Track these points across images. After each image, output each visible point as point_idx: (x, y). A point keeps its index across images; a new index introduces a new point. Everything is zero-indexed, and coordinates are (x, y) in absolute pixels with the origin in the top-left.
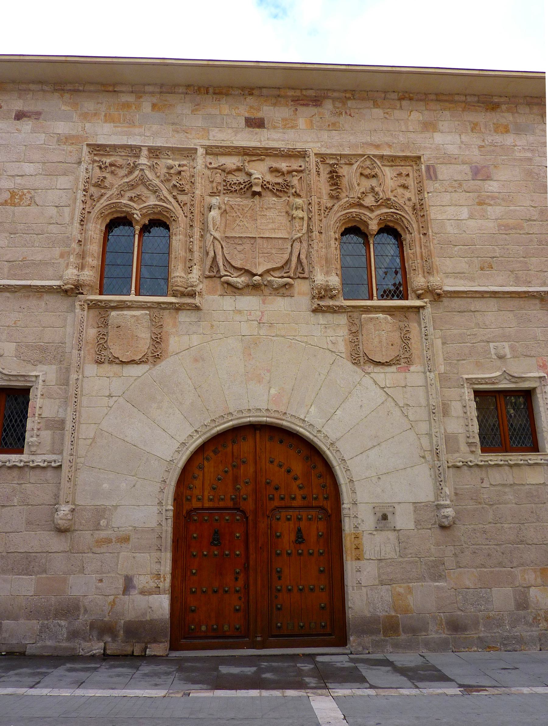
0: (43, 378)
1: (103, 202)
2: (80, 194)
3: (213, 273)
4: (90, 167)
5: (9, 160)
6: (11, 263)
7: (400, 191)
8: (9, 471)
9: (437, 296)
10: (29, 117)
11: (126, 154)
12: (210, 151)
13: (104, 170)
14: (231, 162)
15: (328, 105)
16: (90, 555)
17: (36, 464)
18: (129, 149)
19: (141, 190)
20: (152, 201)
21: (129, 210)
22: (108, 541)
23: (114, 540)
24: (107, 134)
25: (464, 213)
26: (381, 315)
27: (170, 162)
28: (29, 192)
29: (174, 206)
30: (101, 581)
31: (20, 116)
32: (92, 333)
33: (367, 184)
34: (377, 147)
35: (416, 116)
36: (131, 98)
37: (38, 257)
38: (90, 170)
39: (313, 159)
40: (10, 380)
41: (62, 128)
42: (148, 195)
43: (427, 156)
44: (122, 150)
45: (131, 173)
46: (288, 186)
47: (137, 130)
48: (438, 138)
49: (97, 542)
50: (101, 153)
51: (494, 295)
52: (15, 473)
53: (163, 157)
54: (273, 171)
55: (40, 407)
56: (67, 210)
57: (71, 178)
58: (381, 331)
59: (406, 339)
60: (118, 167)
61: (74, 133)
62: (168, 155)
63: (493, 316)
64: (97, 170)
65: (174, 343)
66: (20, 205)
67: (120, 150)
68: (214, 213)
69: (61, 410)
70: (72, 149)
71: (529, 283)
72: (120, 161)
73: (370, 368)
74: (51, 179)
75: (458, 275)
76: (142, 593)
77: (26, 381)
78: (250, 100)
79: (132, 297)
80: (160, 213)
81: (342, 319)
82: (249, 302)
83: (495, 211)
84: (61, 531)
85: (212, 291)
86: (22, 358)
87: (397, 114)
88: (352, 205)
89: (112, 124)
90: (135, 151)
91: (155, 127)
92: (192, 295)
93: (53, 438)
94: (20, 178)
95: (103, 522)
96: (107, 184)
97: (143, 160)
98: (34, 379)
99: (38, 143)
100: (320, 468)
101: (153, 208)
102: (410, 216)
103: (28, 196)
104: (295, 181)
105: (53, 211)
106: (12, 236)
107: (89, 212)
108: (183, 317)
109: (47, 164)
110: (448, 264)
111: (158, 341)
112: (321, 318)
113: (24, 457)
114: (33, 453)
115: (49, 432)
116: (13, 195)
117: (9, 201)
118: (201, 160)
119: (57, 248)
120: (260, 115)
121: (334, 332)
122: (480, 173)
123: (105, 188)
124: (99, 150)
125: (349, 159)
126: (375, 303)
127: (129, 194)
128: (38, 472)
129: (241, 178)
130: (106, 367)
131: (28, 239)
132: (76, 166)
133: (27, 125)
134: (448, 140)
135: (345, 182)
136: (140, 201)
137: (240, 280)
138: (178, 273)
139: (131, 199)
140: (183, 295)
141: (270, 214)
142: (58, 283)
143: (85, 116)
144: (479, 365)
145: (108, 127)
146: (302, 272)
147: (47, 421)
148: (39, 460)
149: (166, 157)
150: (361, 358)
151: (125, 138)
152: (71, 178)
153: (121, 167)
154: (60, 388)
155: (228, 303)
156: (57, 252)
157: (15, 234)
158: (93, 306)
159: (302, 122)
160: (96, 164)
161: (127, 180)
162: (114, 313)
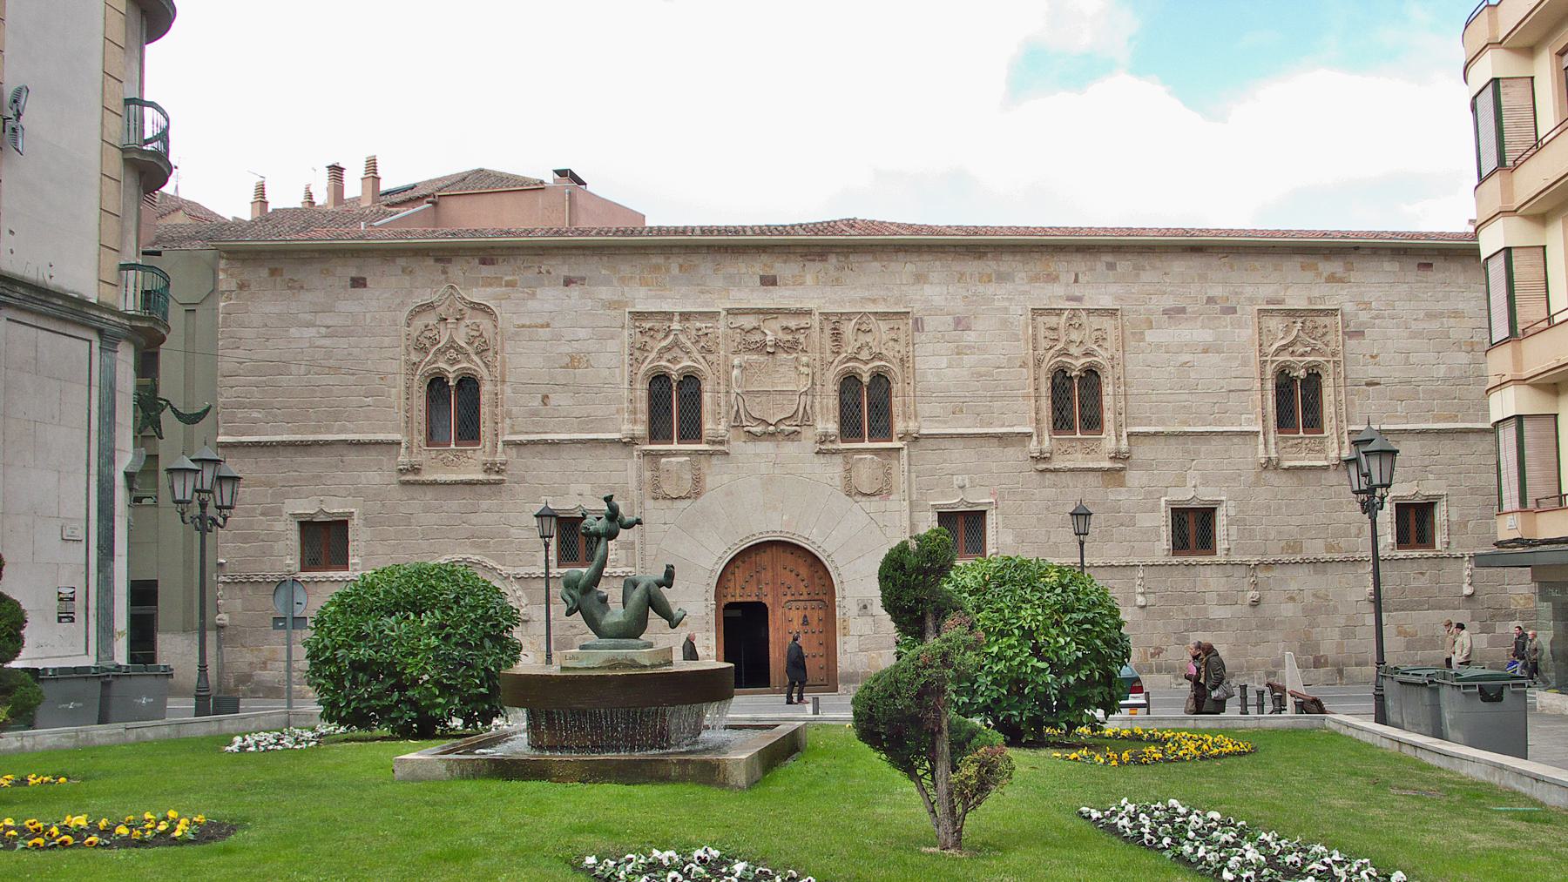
1: (645, 367)
2: (627, 358)
3: (737, 424)
7: (891, 343)
9: (915, 439)
12: (729, 312)
14: (748, 322)
15: (833, 259)
20: (686, 363)
24: (644, 299)
25: (944, 363)
26: (869, 456)
27: (698, 325)
29: (703, 366)
31: (568, 282)
32: (648, 474)
33: (863, 338)
34: (874, 301)
35: (910, 267)
36: (659, 260)
37: (600, 413)
39: (817, 318)
41: (605, 293)
43: (917, 308)
45: (666, 336)
46: (797, 342)
48: (928, 290)
51: (961, 436)
54: (785, 328)
58: (866, 470)
59: (887, 474)
63: (959, 455)
65: (709, 481)
68: (736, 372)
71: (990, 424)
72: (657, 325)
73: (858, 498)
75: (932, 418)
78: (764, 257)
79: (675, 446)
81: (838, 459)
82: (765, 447)
83: (969, 360)
85: (737, 438)
87: (893, 266)
88: (849, 360)
90: (669, 316)
91: (684, 289)
92: (721, 443)
97: (676, 326)
100: (821, 573)
102: (896, 368)
104: (802, 339)
108: (715, 460)
110: (925, 409)
111: (697, 480)
112: (822, 459)
116: (572, 358)
118: (722, 323)
120: (772, 272)
121: (833, 470)
122: (961, 324)
125: (848, 316)
126: (867, 444)
127: (667, 356)
129: (757, 337)
133: (575, 291)
134: (934, 292)
135: (845, 337)
137: (758, 429)
138: (708, 426)
140: (714, 442)
141: (782, 370)
143: (622, 280)
144: (943, 494)
145: (643, 291)
146: (807, 420)
150: (852, 491)
155: (752, 448)
156: (613, 408)
158: (646, 454)
159: (809, 279)
161: (664, 343)
162: (663, 460)
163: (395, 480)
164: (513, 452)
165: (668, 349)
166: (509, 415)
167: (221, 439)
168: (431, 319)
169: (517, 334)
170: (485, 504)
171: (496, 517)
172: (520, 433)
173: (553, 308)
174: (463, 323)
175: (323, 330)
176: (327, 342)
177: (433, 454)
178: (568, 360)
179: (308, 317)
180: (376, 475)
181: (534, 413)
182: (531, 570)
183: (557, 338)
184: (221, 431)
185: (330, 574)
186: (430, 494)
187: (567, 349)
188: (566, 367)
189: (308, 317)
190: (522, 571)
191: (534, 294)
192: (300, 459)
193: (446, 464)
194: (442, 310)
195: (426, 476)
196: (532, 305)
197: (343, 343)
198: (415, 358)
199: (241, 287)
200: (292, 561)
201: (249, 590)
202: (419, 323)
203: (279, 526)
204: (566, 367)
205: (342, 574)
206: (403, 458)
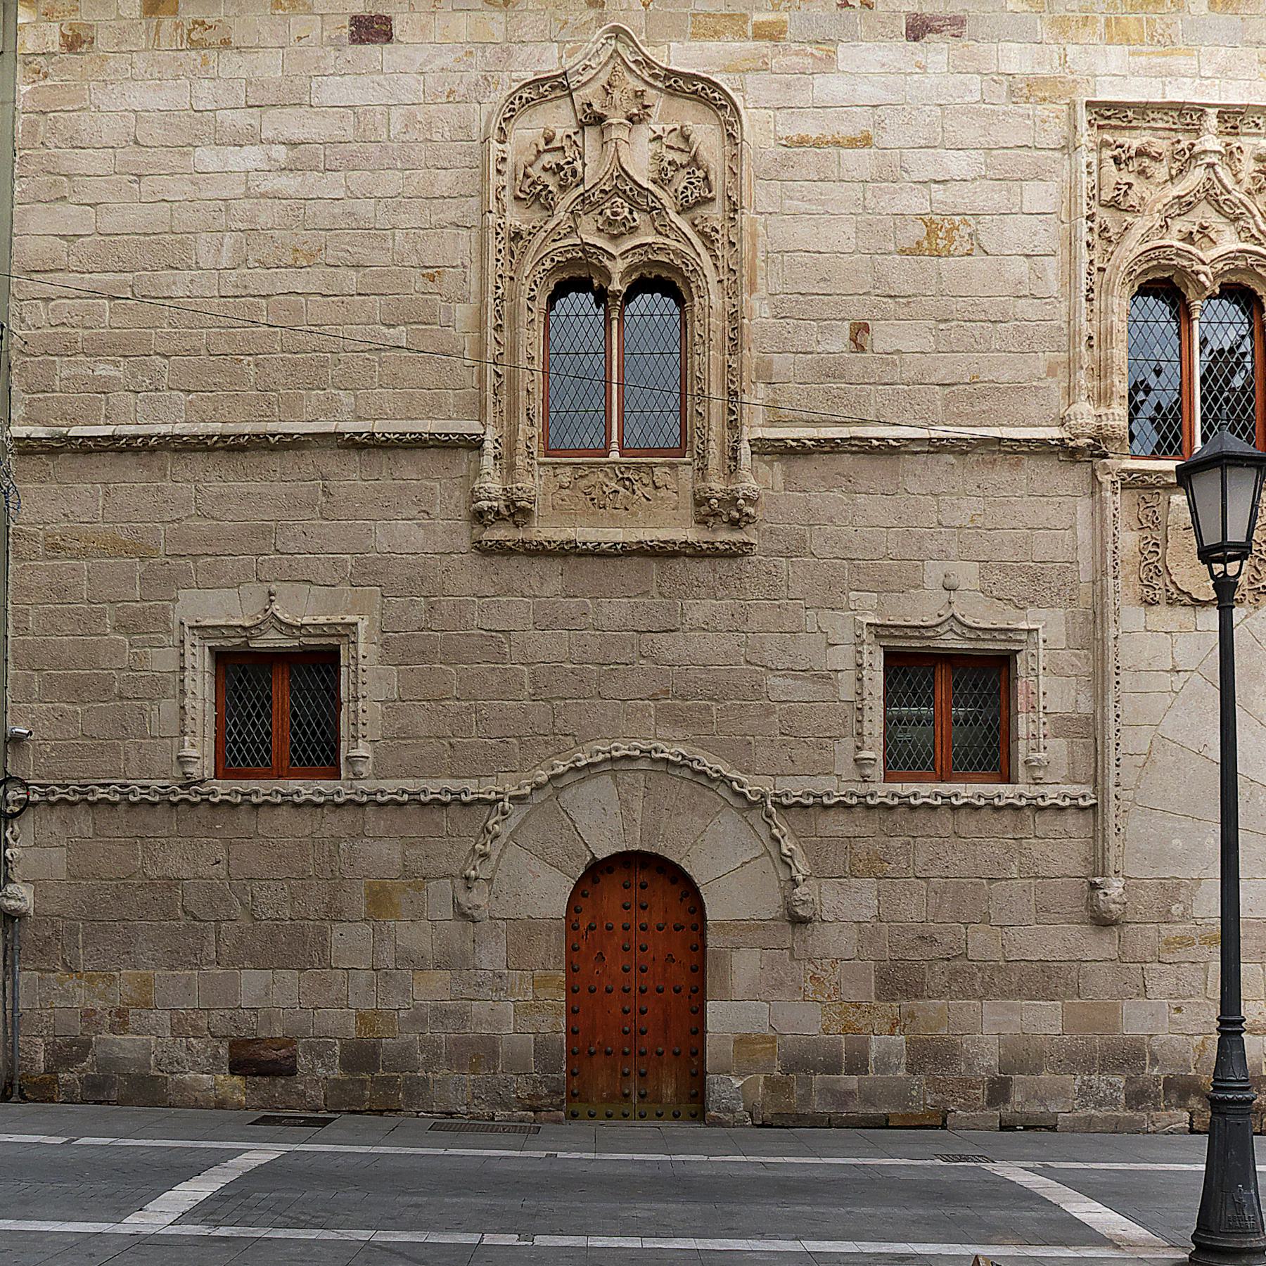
0: (1045, 633)
1: (1132, 247)
4: (1093, 158)
5: (911, 144)
6: (947, 390)
8: (995, 816)
10: (939, 31)
11: (1167, 126)
13: (1123, 166)
16: (1155, 965)
17: (1048, 802)
18: (1175, 114)
19: (1205, 214)
20: (1229, 242)
21: (1186, 263)
22: (1185, 942)
23: (1196, 940)
24: (1121, 76)
28: (966, 223)
30: (1179, 1010)
31: (918, 29)
32: (1129, 540)
38: (1094, 167)
40: (978, 639)
42: (1221, 227)
44: (1159, 116)
47: (1180, 62)
49: (1167, 943)
50: (1113, 122)
52: (1007, 818)
53: (1245, 130)
55: (1046, 692)
56: (1051, 266)
57: (1053, 186)
60: (1154, 158)
61: (1045, 71)
62: (1257, 125)
64: (1110, 166)
66: (950, 255)
67: (1155, 115)
69: (1081, 698)
70: (1046, 113)
74: (1009, 191)
77: (1009, 640)
80: (1250, 270)
84: (1102, 922)
86: (995, 593)
89: (1126, 48)
93: (1071, 753)
94: (941, 187)
95: (1176, 909)
96: (1133, 199)
98: (1024, 637)
99: (967, 99)
101: (1235, 258)
103: (965, 230)
105: (1021, 267)
106: (942, 326)
107: (1101, 270)
109: (994, 152)
113: (1020, 788)
114: (1036, 782)
115: (1062, 742)
116: (932, 229)
117: (925, 244)
119: (1040, 354)
123: (1131, 209)
124: (1109, 118)
128: (1048, 816)
130: (1162, 610)
131: (976, 333)
132: (1057, 155)
136: (1206, 239)
139: (1189, 238)
142: (1055, 433)
147: (1057, 719)
148: (1052, 794)
149: (1255, 130)
151: (1157, 82)
152: (1053, 186)
153: (1157, 158)
154: (1076, 655)
156: (1041, 362)
157: (946, 321)
160: (1107, 153)
163: (464, 543)
164: (776, 471)
165: (1185, 205)
166: (766, 375)
167: (18, 431)
168: (558, 119)
169: (784, 163)
170: (700, 610)
171: (728, 643)
172: (792, 422)
173: (880, 95)
174: (643, 133)
175: (280, 153)
176: (287, 183)
177: (566, 476)
178: (919, 231)
179: (242, 119)
180: (414, 523)
181: (830, 371)
182: (822, 785)
183: (889, 176)
184: (18, 411)
185: (294, 784)
186: (550, 580)
187: (914, 202)
188: (915, 251)
189: (242, 119)
190: (796, 787)
191: (830, 59)
192: (216, 487)
193: (598, 503)
194: (590, 94)
195: (543, 531)
196: (829, 87)
197: (332, 185)
198: (516, 218)
199: (73, 43)
200: (200, 751)
201: (84, 823)
202: (527, 131)
203: (162, 660)
204: (915, 251)
205: (324, 785)
206: (492, 484)
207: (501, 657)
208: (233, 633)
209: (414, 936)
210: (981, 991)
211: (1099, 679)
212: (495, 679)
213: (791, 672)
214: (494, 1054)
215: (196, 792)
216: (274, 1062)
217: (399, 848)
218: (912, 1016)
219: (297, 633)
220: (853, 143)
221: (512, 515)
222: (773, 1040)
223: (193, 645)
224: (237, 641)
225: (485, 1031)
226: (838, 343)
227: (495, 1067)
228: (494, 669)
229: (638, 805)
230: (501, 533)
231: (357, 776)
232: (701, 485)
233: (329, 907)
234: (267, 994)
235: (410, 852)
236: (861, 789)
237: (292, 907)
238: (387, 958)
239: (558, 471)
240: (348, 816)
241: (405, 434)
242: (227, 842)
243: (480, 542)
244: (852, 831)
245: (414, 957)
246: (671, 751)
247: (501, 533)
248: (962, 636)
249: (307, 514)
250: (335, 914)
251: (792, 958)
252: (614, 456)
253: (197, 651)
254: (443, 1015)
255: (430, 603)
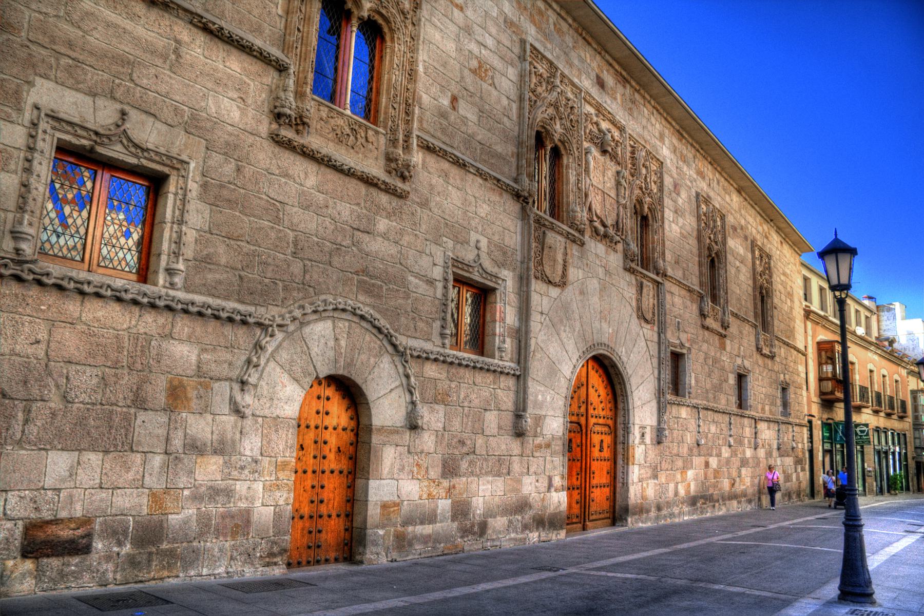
76: (556, 490)
113: (496, 361)
195: (314, 141)
207: (277, 220)
208: (84, 134)
209: (200, 427)
210: (478, 472)
211: (524, 311)
212: (273, 235)
213: (417, 276)
214: (248, 522)
215: (30, 270)
216: (72, 541)
217: (196, 352)
218: (454, 487)
219: (140, 154)
220: (457, 6)
221: (297, 124)
222: (398, 505)
223: (45, 132)
224: (85, 142)
225: (243, 505)
226: (446, 102)
227: (248, 534)
228: (272, 228)
229: (343, 343)
230: (287, 133)
231: (172, 285)
232: (391, 149)
233: (137, 395)
234: (71, 475)
235: (206, 356)
236: (442, 350)
237: (104, 394)
238: (177, 443)
239: (322, 108)
240: (163, 319)
241: (242, 39)
242: (52, 323)
243: (277, 135)
244: (438, 376)
245: (199, 444)
246: (366, 310)
247: (287, 133)
248: (481, 275)
249: (159, 62)
250: (139, 402)
251: (409, 452)
252: (348, 112)
253: (47, 137)
254: (215, 493)
255: (237, 165)
